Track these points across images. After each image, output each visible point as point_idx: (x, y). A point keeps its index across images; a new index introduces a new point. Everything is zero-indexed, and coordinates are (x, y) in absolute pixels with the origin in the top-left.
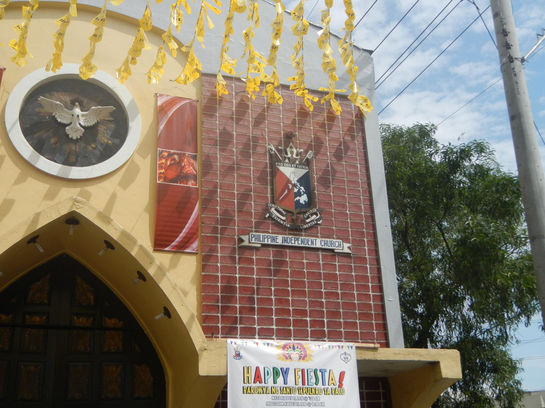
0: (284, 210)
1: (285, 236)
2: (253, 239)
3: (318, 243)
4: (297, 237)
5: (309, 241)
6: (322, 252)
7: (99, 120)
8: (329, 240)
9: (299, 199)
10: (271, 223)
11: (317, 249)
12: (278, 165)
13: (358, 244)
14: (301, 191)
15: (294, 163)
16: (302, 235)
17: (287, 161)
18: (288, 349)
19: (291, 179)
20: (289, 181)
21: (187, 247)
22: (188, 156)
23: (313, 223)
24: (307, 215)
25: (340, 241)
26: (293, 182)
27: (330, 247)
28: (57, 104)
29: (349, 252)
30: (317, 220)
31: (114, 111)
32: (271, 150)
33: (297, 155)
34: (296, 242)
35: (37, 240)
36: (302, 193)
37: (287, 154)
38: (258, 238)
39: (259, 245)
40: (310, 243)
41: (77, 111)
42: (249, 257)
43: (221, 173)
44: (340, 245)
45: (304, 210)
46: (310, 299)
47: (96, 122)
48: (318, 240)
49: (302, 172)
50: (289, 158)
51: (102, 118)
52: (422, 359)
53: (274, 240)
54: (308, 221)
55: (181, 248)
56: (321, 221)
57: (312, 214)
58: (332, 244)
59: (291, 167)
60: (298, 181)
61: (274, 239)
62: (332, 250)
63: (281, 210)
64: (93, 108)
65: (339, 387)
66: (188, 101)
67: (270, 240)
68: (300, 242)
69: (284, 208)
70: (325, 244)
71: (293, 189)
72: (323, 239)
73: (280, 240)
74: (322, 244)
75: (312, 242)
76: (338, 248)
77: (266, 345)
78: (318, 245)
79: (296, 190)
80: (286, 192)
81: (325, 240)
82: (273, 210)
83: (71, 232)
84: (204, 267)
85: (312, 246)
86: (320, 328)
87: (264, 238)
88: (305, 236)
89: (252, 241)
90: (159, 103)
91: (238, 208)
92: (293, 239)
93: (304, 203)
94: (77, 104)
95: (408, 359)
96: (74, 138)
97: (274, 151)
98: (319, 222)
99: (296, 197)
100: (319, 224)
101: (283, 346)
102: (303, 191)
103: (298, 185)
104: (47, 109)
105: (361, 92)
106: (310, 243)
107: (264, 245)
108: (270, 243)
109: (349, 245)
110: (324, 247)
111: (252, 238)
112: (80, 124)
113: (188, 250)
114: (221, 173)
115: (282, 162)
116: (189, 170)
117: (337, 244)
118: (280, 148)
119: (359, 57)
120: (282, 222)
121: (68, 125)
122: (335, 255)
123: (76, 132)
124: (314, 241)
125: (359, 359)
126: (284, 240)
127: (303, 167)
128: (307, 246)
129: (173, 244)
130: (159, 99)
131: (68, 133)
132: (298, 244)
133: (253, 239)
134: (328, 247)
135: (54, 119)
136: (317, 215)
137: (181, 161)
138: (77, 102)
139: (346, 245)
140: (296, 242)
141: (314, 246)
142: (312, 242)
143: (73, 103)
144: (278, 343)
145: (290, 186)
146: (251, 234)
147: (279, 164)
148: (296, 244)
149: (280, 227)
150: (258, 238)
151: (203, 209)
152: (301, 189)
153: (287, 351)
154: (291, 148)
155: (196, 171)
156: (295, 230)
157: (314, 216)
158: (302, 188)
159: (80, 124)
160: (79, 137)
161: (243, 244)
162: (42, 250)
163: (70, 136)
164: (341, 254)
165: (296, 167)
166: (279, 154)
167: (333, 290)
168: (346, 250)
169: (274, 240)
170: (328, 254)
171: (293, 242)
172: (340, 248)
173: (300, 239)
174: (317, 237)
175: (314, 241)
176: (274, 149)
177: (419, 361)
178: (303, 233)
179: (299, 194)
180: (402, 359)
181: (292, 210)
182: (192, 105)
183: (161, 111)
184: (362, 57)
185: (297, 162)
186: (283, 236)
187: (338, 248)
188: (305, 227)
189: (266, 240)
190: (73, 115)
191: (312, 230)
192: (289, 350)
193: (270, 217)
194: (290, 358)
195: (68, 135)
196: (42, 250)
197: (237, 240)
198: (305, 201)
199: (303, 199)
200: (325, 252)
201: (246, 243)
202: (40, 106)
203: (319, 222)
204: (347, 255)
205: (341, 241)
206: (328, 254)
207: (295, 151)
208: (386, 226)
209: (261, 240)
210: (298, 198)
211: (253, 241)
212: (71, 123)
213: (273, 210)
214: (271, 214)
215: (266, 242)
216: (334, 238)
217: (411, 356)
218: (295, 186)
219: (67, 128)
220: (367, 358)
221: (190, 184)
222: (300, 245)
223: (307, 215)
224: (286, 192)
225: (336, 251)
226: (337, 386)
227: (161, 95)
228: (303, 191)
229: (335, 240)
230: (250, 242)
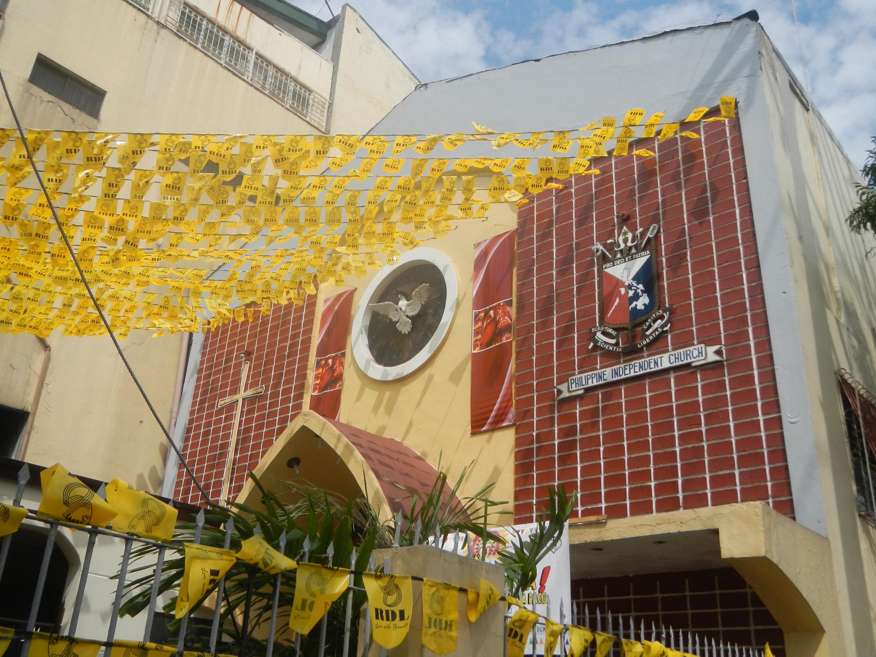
0: (615, 329)
1: (616, 367)
2: (574, 385)
3: (665, 361)
4: (633, 363)
5: (650, 362)
6: (675, 372)
7: (423, 303)
8: (682, 351)
9: (636, 305)
10: (601, 354)
11: (666, 371)
12: (606, 268)
13: (737, 338)
14: (639, 291)
15: (628, 255)
16: (643, 357)
17: (619, 256)
19: (624, 279)
20: (618, 283)
21: (503, 421)
22: (503, 306)
23: (657, 333)
24: (647, 324)
25: (699, 346)
26: (626, 284)
27: (685, 362)
28: (386, 305)
29: (717, 358)
30: (663, 326)
31: (429, 286)
32: (598, 250)
33: (633, 241)
34: (632, 371)
36: (640, 294)
37: (619, 246)
38: (579, 382)
39: (581, 392)
40: (652, 365)
41: (403, 303)
44: (702, 353)
45: (643, 318)
46: (656, 452)
47: (420, 305)
48: (666, 356)
49: (640, 262)
50: (621, 251)
51: (426, 300)
52: (684, 529)
53: (600, 377)
54: (648, 333)
55: (497, 425)
56: (669, 325)
57: (655, 321)
58: (687, 355)
59: (625, 261)
60: (633, 279)
61: (600, 377)
62: (688, 366)
63: (610, 331)
64: (414, 293)
65: (539, 592)
66: (507, 235)
67: (595, 380)
68: (637, 369)
69: (614, 326)
70: (676, 359)
71: (627, 293)
72: (673, 353)
73: (608, 375)
74: (672, 361)
75: (656, 363)
76: (698, 359)
78: (666, 364)
79: (631, 293)
80: (617, 300)
81: (676, 352)
82: (599, 335)
84: (518, 442)
85: (657, 369)
86: (670, 494)
87: (588, 379)
88: (648, 356)
92: (628, 367)
93: (643, 308)
94: (399, 296)
95: (658, 533)
96: (407, 332)
97: (602, 250)
98: (665, 329)
99: (631, 303)
100: (666, 331)
102: (642, 291)
103: (635, 285)
105: (737, 88)
106: (652, 365)
107: (587, 390)
108: (595, 383)
109: (716, 347)
110: (674, 364)
111: (572, 384)
112: (407, 316)
113: (505, 424)
115: (613, 261)
116: (504, 321)
117: (696, 353)
118: (609, 241)
119: (730, 33)
120: (611, 348)
121: (398, 322)
122: (695, 373)
123: (405, 327)
124: (659, 360)
125: (576, 542)
126: (616, 373)
127: (643, 253)
128: (649, 370)
129: (489, 421)
132: (635, 372)
133: (574, 385)
134: (681, 363)
135: (391, 320)
136: (662, 317)
137: (496, 314)
139: (711, 349)
140: (632, 371)
141: (660, 368)
142: (656, 363)
145: (623, 291)
146: (570, 379)
147: (608, 265)
148: (633, 374)
149: (611, 357)
150: (579, 382)
151: (518, 367)
152: (638, 288)
154: (625, 233)
155: (511, 320)
156: (632, 352)
157: (659, 321)
158: (641, 287)
159: (407, 316)
160: (410, 330)
161: (562, 396)
163: (403, 333)
164: (706, 367)
165: (632, 259)
166: (608, 251)
167: (693, 428)
168: (712, 357)
169: (600, 377)
170: (683, 373)
171: (627, 372)
172: (701, 358)
173: (638, 364)
174: (667, 351)
175: (659, 360)
176: (601, 247)
177: (679, 533)
178: (645, 354)
179: (636, 297)
180: (647, 534)
181: (625, 326)
182: (510, 237)
183: (478, 264)
184: (733, 33)
185: (633, 251)
186: (613, 368)
187: (698, 359)
188: (645, 343)
189: (590, 381)
191: (657, 344)
193: (596, 347)
198: (645, 305)
199: (642, 302)
200: (680, 371)
201: (566, 394)
203: (665, 329)
204: (716, 366)
205: (703, 345)
206: (683, 373)
207: (630, 236)
208: (784, 293)
209: (584, 383)
210: (633, 305)
211: (574, 388)
213: (599, 335)
214: (596, 341)
215: (590, 384)
216: (693, 345)
217: (663, 526)
218: (630, 287)
220: (589, 540)
221: (504, 340)
222: (639, 373)
223: (647, 324)
224: (617, 300)
225: (694, 364)
226: (537, 591)
227: (479, 244)
228: (642, 291)
229: (691, 348)
230: (569, 391)
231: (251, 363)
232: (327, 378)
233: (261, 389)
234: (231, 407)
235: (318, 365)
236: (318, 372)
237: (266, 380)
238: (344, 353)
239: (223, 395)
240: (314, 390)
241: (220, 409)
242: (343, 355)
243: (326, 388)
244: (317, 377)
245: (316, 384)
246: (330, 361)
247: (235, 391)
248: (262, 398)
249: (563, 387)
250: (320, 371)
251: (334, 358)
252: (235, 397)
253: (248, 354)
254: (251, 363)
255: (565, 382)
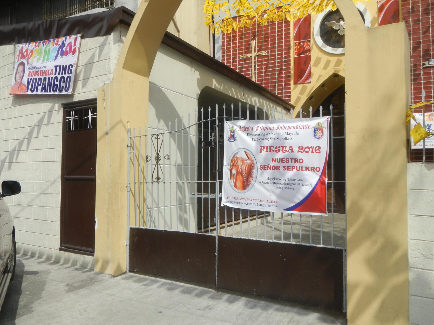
18: (432, 116)
35: (325, 86)
42: (429, 71)
43: (413, 32)
77: (420, 116)
83: (336, 80)
89: (430, 63)
90: (379, 6)
91: (422, 48)
94: (341, 20)
101: (429, 115)
104: (330, 25)
114: (413, 32)
130: (378, 4)
131: (339, 34)
135: (333, 29)
138: (341, 19)
143: (339, 19)
144: (427, 114)
153: (431, 117)
162: (326, 89)
163: (340, 35)
183: (380, 9)
190: (340, 25)
192: (432, 117)
194: (432, 120)
195: (339, 34)
196: (326, 89)
197: (422, 64)
202: (326, 25)
212: (340, 29)
219: (338, 31)
230: (429, 64)
231: (256, 41)
232: (302, 50)
233: (263, 53)
234: (247, 59)
235: (295, 45)
236: (296, 47)
237: (266, 49)
238: (310, 40)
239: (242, 53)
240: (295, 54)
241: (240, 59)
242: (309, 41)
243: (300, 54)
244: (295, 50)
245: (295, 52)
246: (302, 43)
247: (247, 52)
248: (265, 56)
249: (426, 63)
250: (297, 47)
251: (303, 42)
252: (249, 55)
253: (254, 36)
254: (256, 41)
255: (427, 61)
